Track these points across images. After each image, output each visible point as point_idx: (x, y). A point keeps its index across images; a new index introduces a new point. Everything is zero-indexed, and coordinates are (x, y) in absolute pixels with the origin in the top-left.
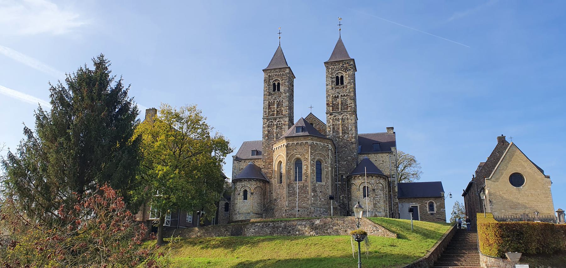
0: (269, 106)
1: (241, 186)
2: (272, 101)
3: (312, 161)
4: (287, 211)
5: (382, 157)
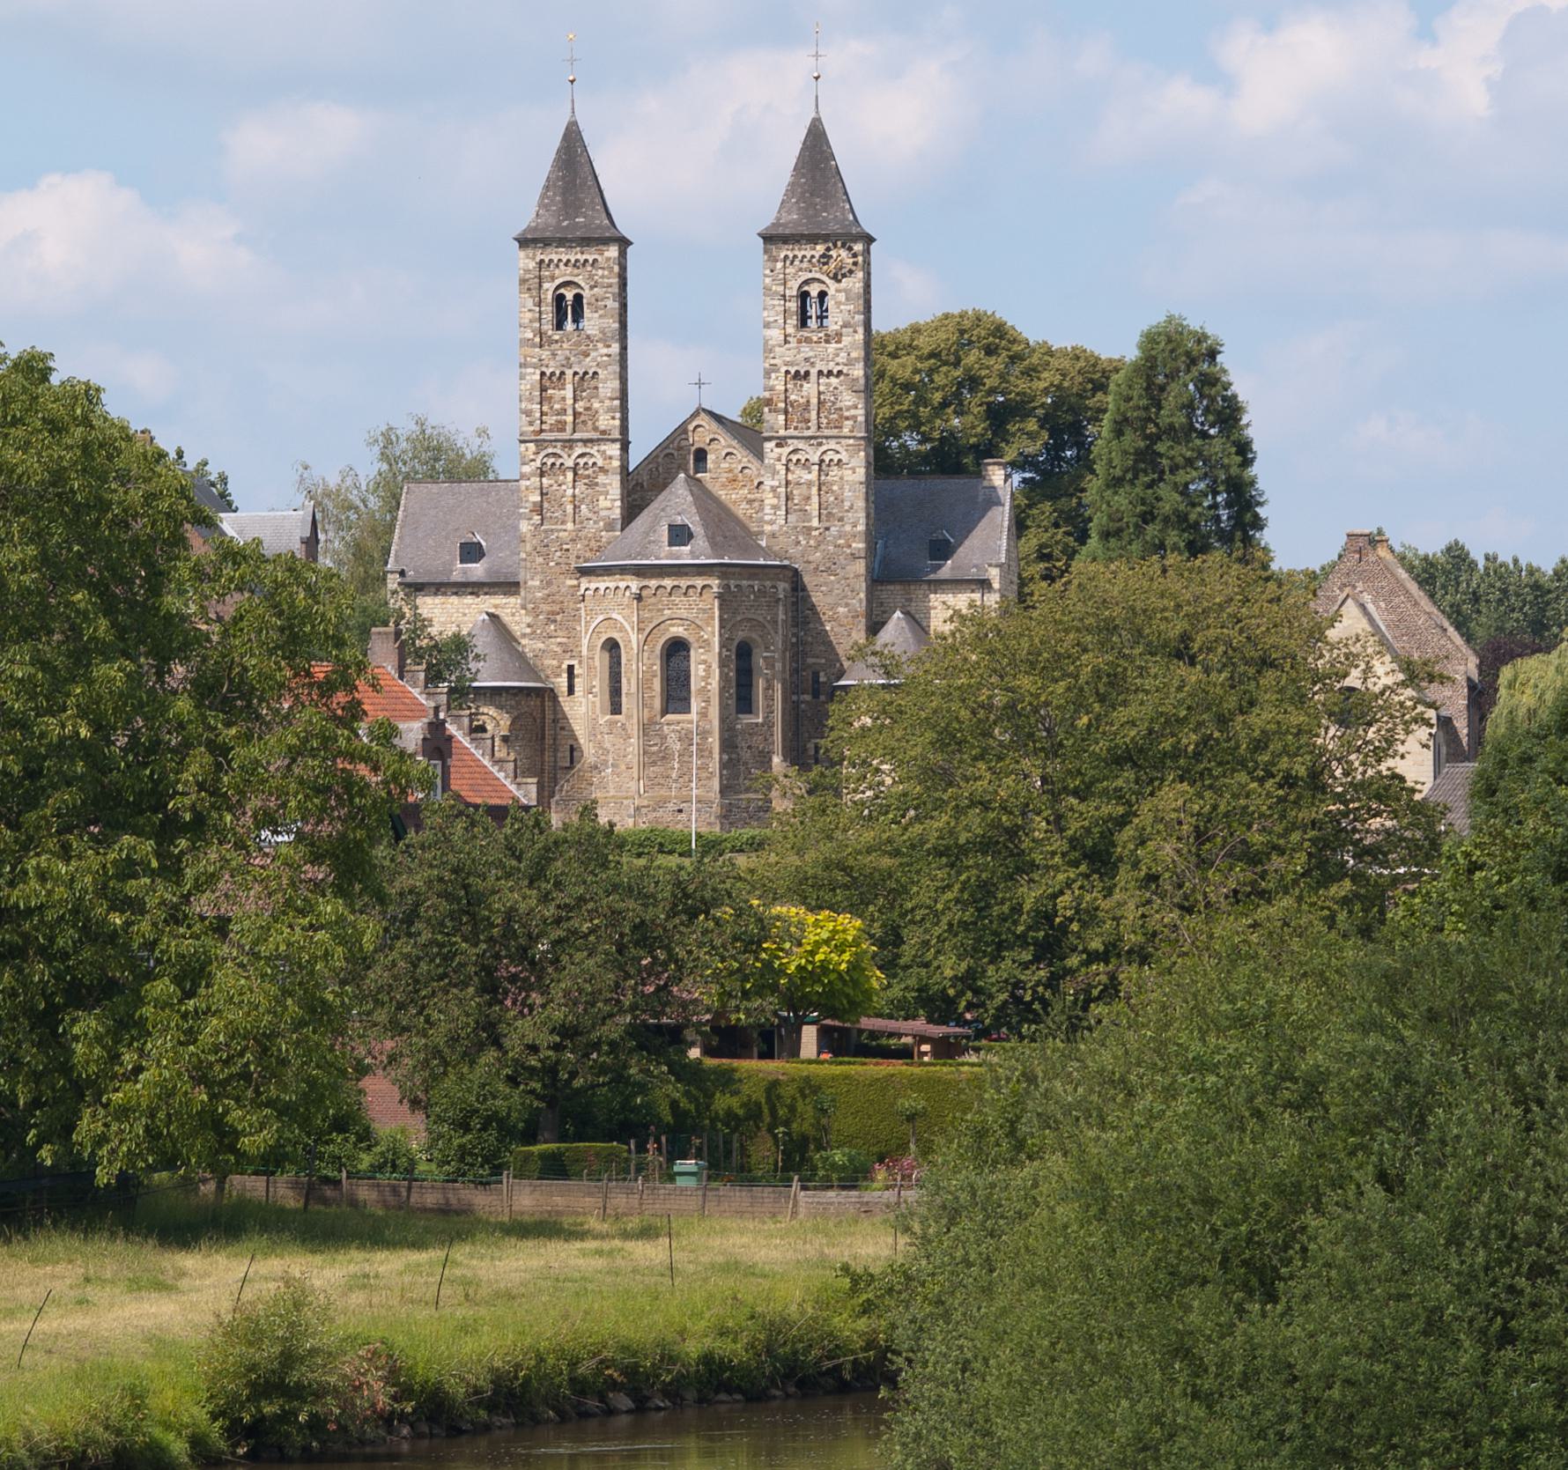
0: (543, 389)
4: (644, 811)
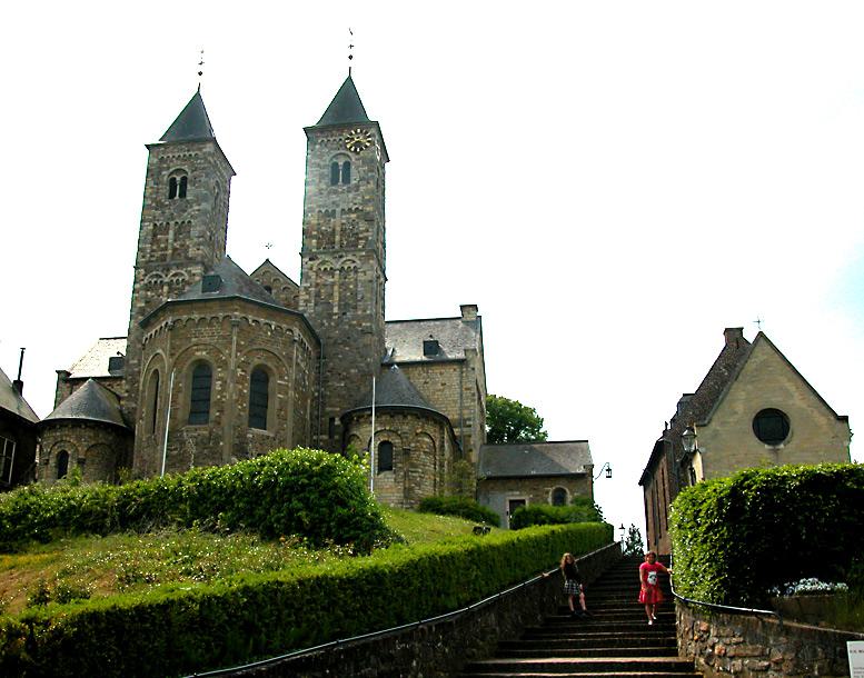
0: (155, 235)
1: (51, 441)
3: (239, 370)
5: (441, 374)
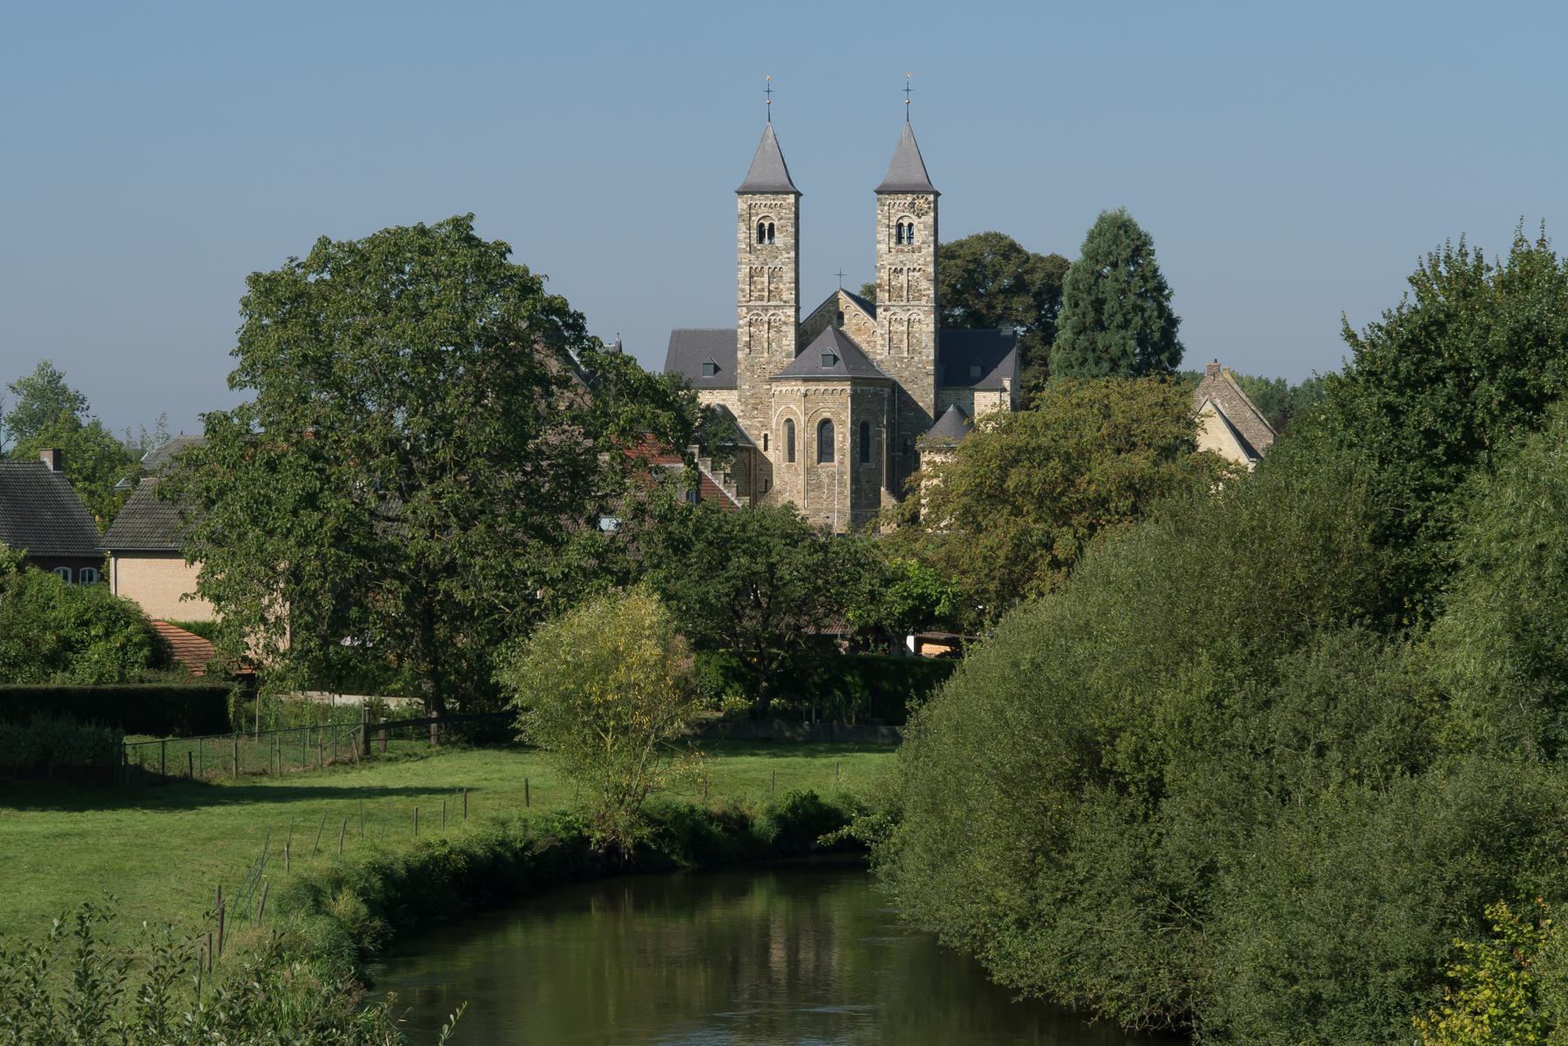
0: (751, 277)
2: (756, 265)
